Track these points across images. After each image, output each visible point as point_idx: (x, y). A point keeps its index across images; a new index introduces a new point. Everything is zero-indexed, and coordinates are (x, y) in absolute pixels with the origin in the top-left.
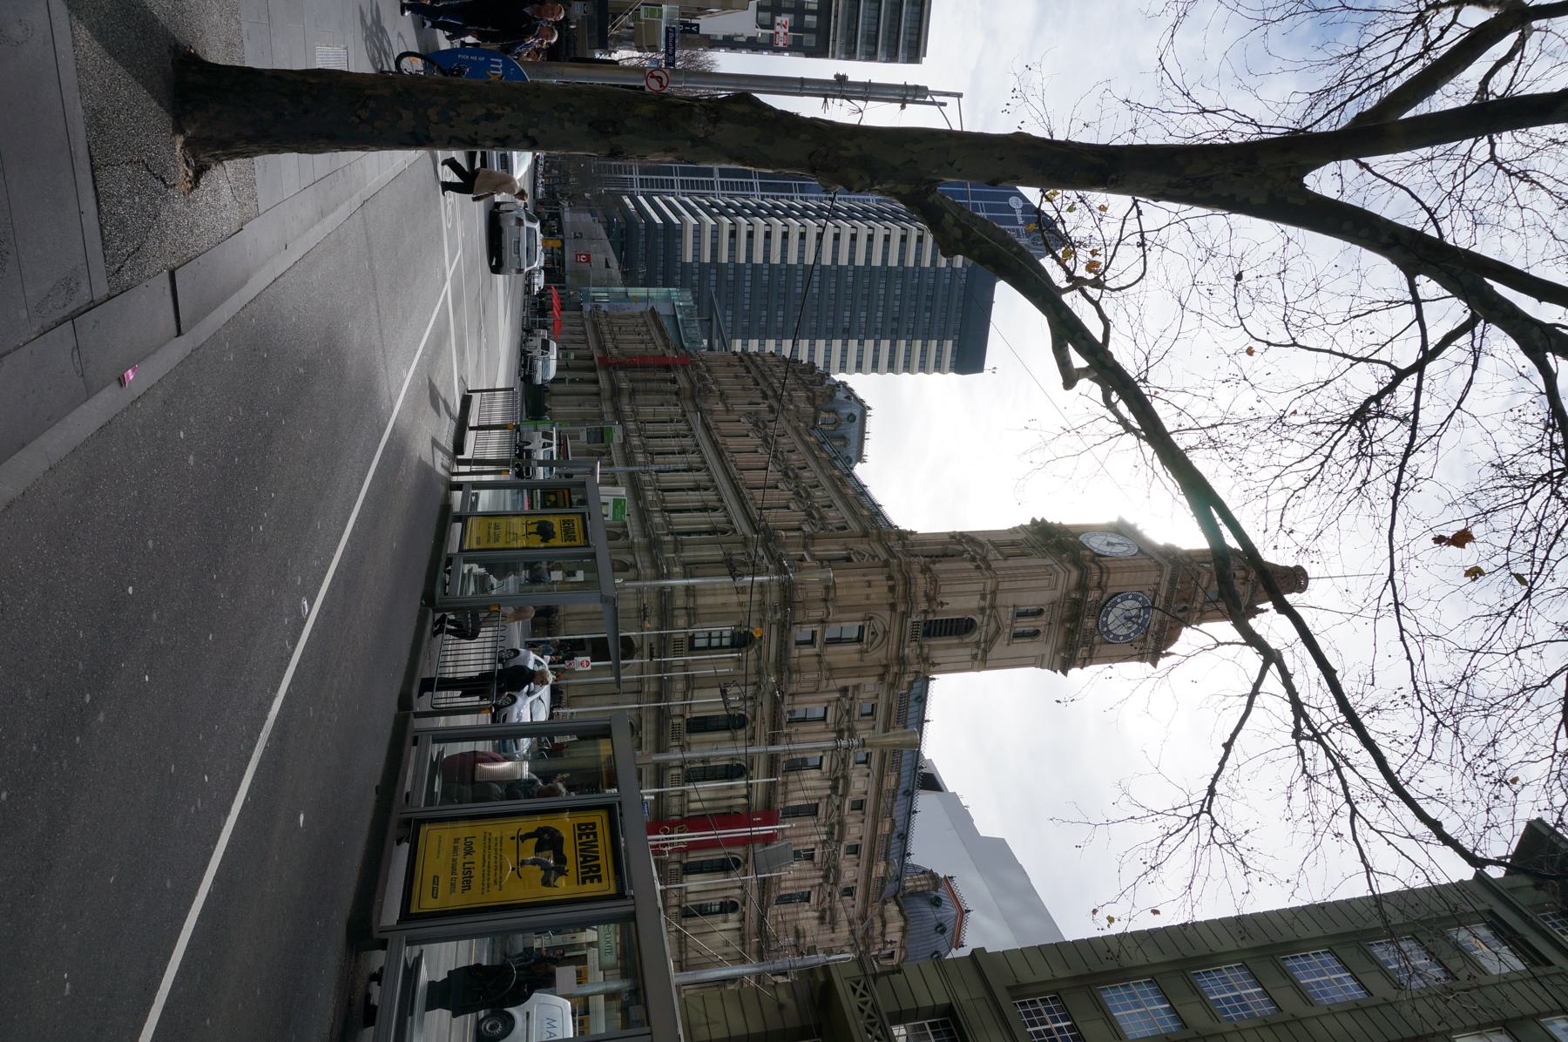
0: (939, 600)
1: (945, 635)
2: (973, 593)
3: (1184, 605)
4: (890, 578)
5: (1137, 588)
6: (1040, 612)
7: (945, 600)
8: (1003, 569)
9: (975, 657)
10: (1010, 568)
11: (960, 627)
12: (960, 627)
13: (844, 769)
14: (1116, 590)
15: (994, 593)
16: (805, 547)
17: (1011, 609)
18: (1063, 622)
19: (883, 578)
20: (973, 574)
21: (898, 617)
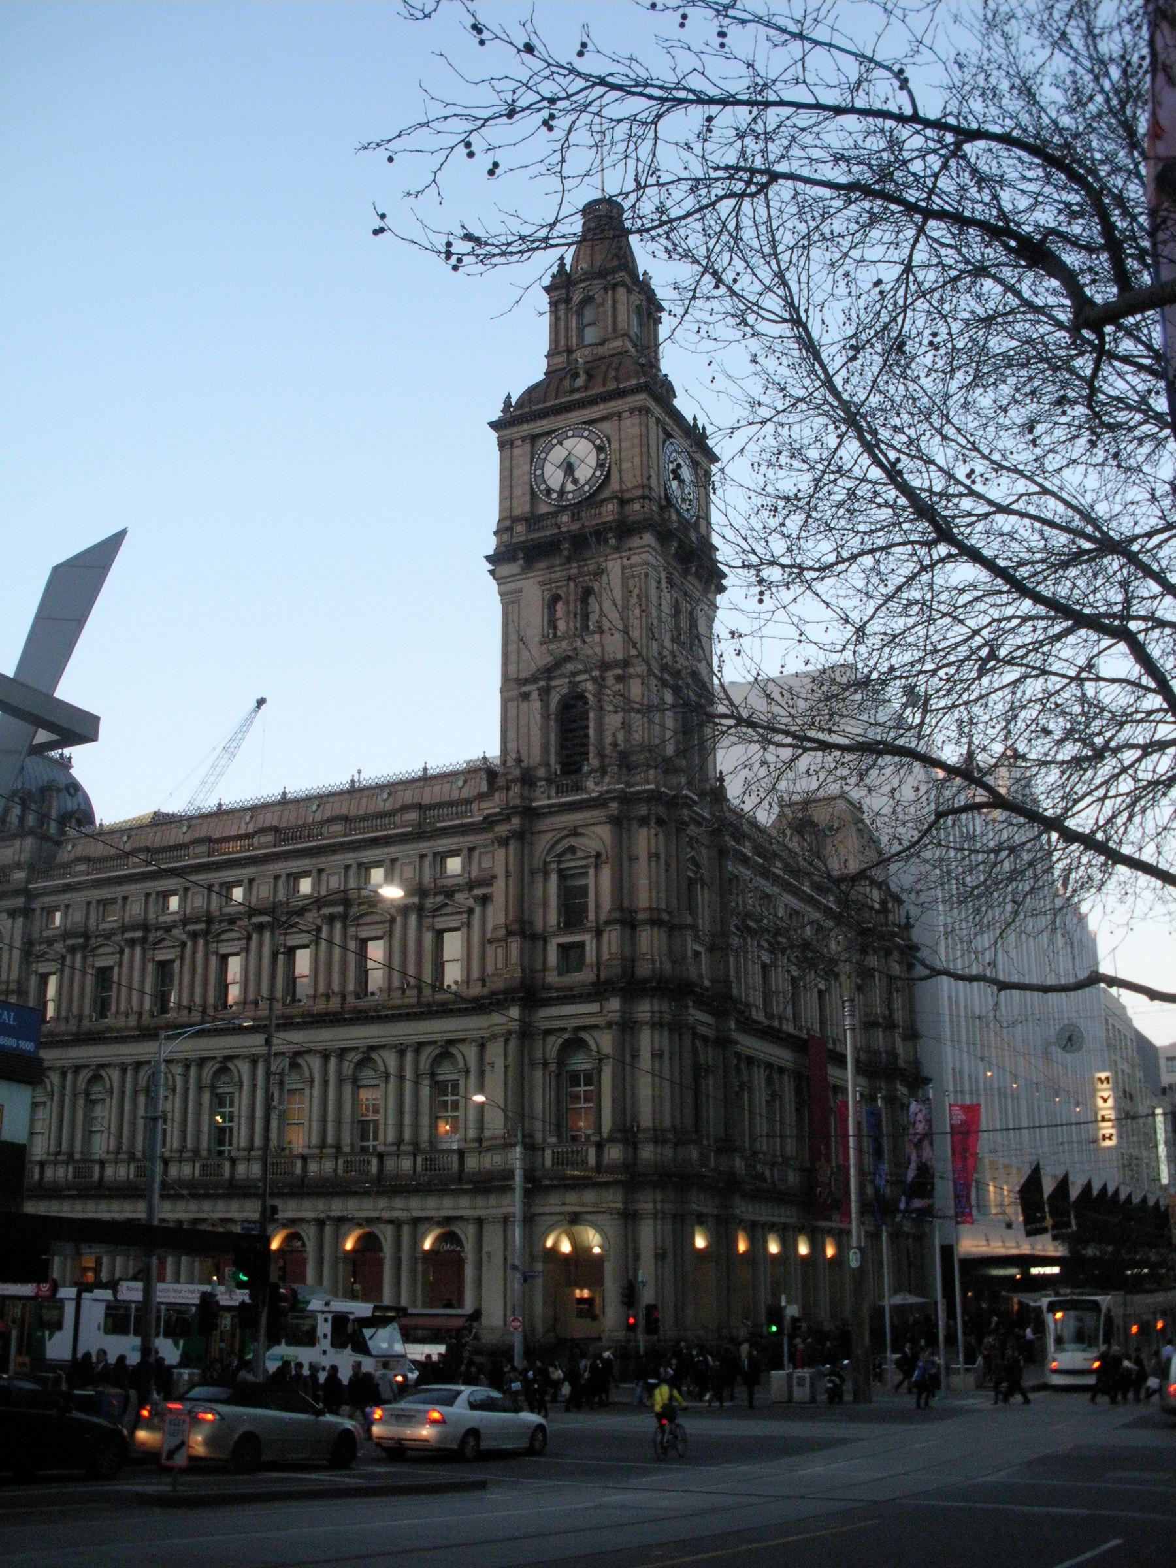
18: (685, 572)
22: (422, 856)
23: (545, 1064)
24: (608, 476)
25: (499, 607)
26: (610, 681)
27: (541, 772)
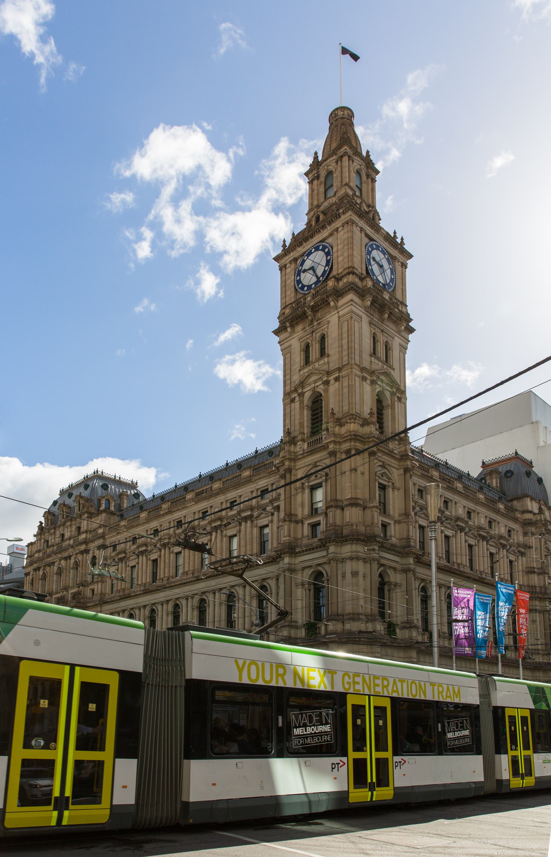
2: (361, 387)
5: (363, 249)
15: (363, 369)
20: (346, 384)
26: (332, 382)
27: (299, 438)
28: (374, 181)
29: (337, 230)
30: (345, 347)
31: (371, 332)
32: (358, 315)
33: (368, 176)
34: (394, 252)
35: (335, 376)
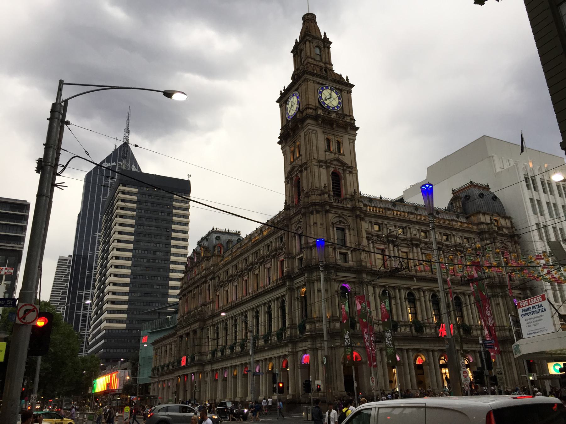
0: (323, 188)
1: (339, 187)
2: (319, 172)
3: (323, 70)
4: (312, 213)
5: (316, 92)
6: (328, 141)
7: (323, 185)
8: (306, 156)
9: (351, 172)
10: (306, 153)
11: (336, 179)
12: (336, 179)
13: (407, 240)
14: (317, 102)
15: (319, 161)
16: (293, 258)
17: (327, 153)
18: (332, 128)
19: (312, 216)
20: (309, 171)
21: (332, 209)
22: (276, 239)
23: (298, 299)
24: (299, 106)
25: (283, 157)
26: (304, 170)
28: (329, 48)
29: (301, 84)
30: (308, 150)
31: (325, 138)
32: (315, 130)
33: (324, 47)
34: (340, 87)
35: (304, 167)
